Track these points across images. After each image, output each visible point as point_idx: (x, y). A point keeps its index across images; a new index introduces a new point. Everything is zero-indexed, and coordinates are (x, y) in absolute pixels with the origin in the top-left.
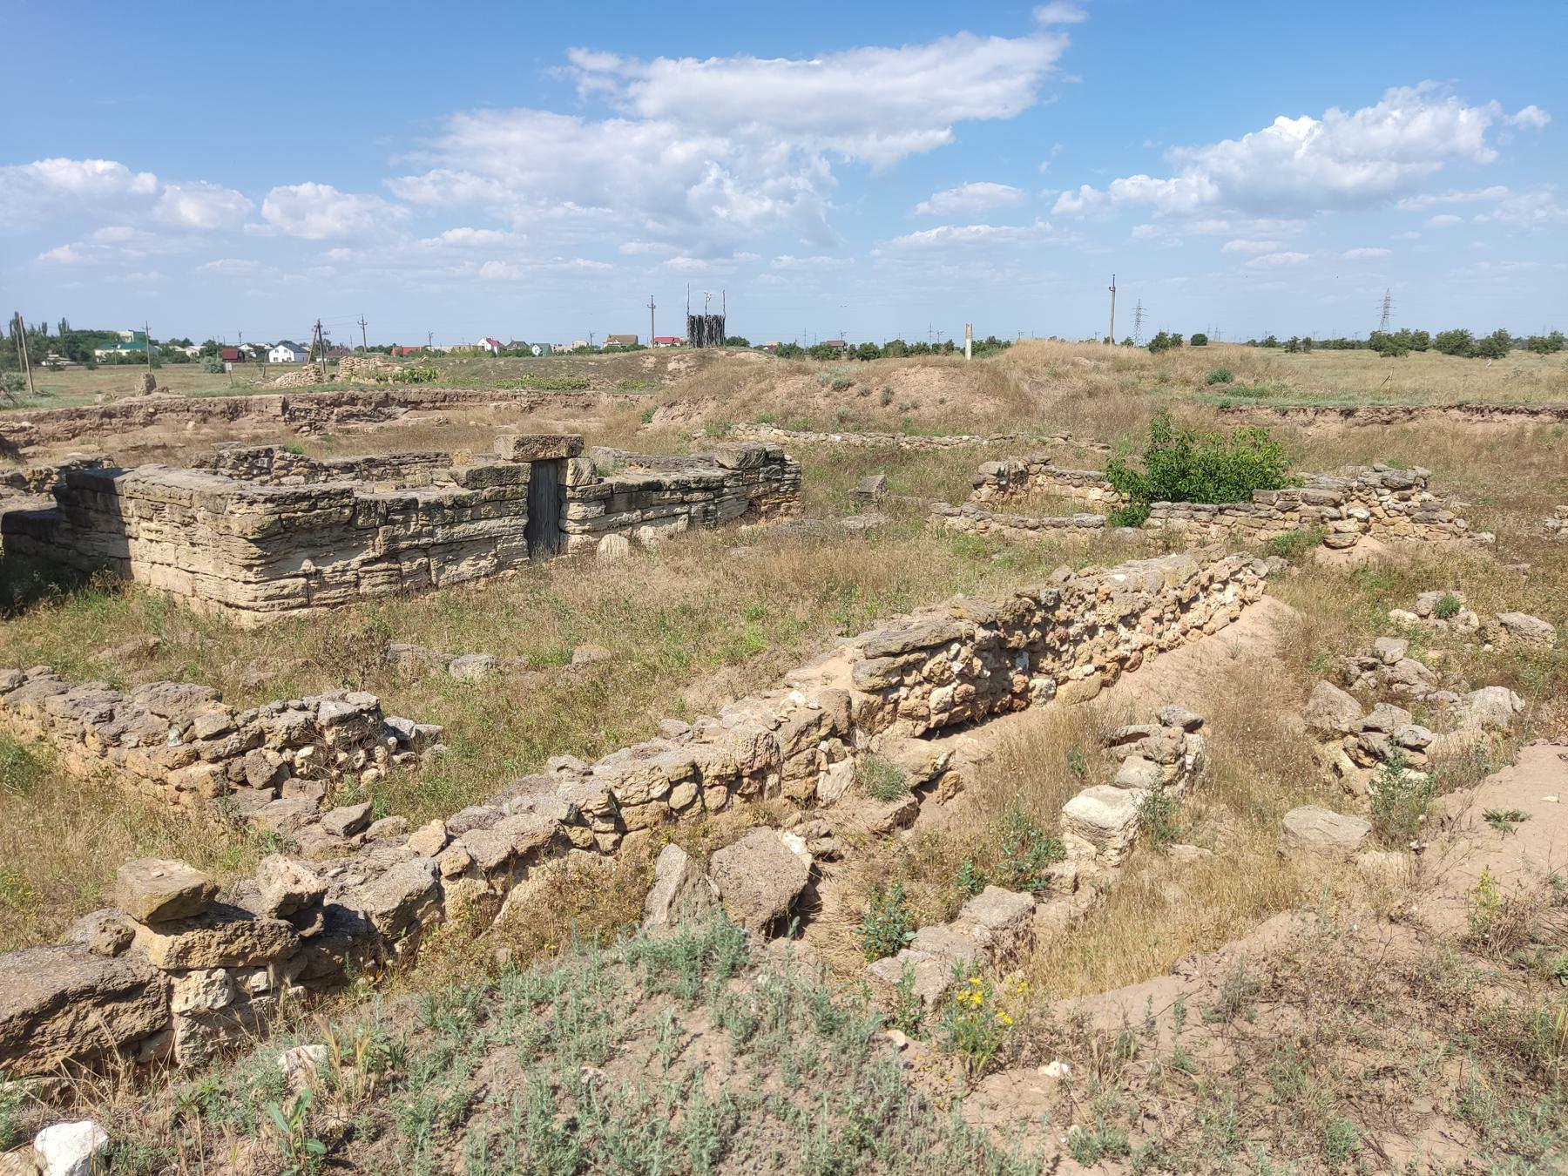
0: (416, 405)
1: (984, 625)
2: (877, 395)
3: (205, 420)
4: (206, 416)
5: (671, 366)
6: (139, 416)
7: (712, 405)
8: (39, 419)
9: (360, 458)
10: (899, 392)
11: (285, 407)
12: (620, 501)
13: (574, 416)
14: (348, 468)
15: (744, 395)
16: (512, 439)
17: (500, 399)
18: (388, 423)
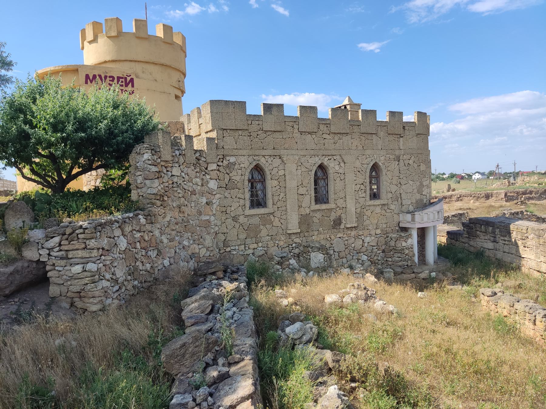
6: (454, 198)
11: (506, 195)
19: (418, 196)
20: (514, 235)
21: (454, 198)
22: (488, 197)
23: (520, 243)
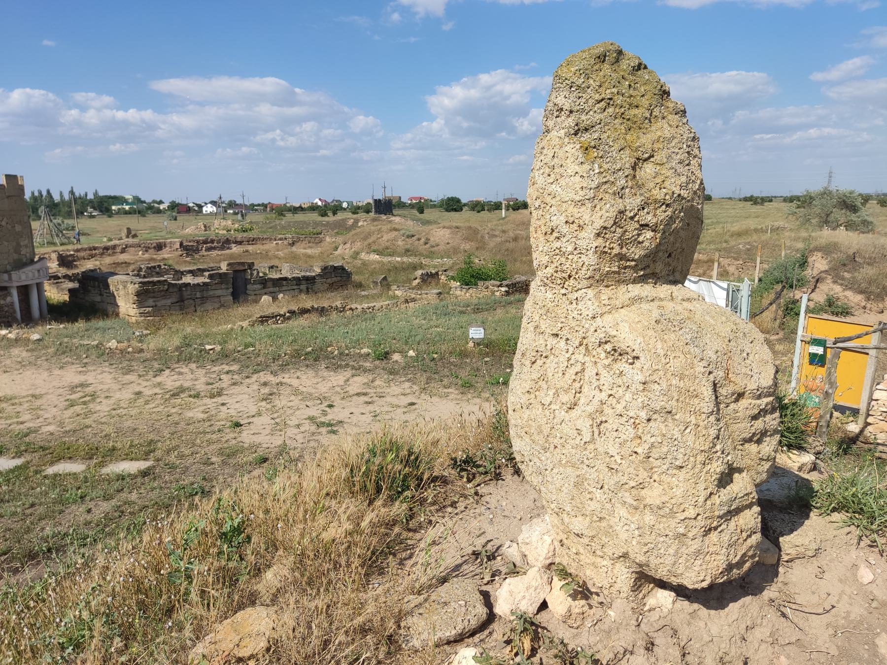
0: (240, 243)
1: (288, 312)
2: (423, 240)
3: (147, 251)
4: (147, 249)
5: (360, 224)
6: (118, 250)
7: (359, 244)
8: (78, 251)
9: (195, 268)
10: (432, 239)
11: (181, 244)
12: (269, 284)
13: (311, 247)
14: (190, 272)
15: (370, 240)
16: (226, 263)
17: (281, 239)
18: (228, 251)
19: (16, 256)
20: (111, 287)
21: (118, 250)
22: (159, 247)
23: (115, 293)
